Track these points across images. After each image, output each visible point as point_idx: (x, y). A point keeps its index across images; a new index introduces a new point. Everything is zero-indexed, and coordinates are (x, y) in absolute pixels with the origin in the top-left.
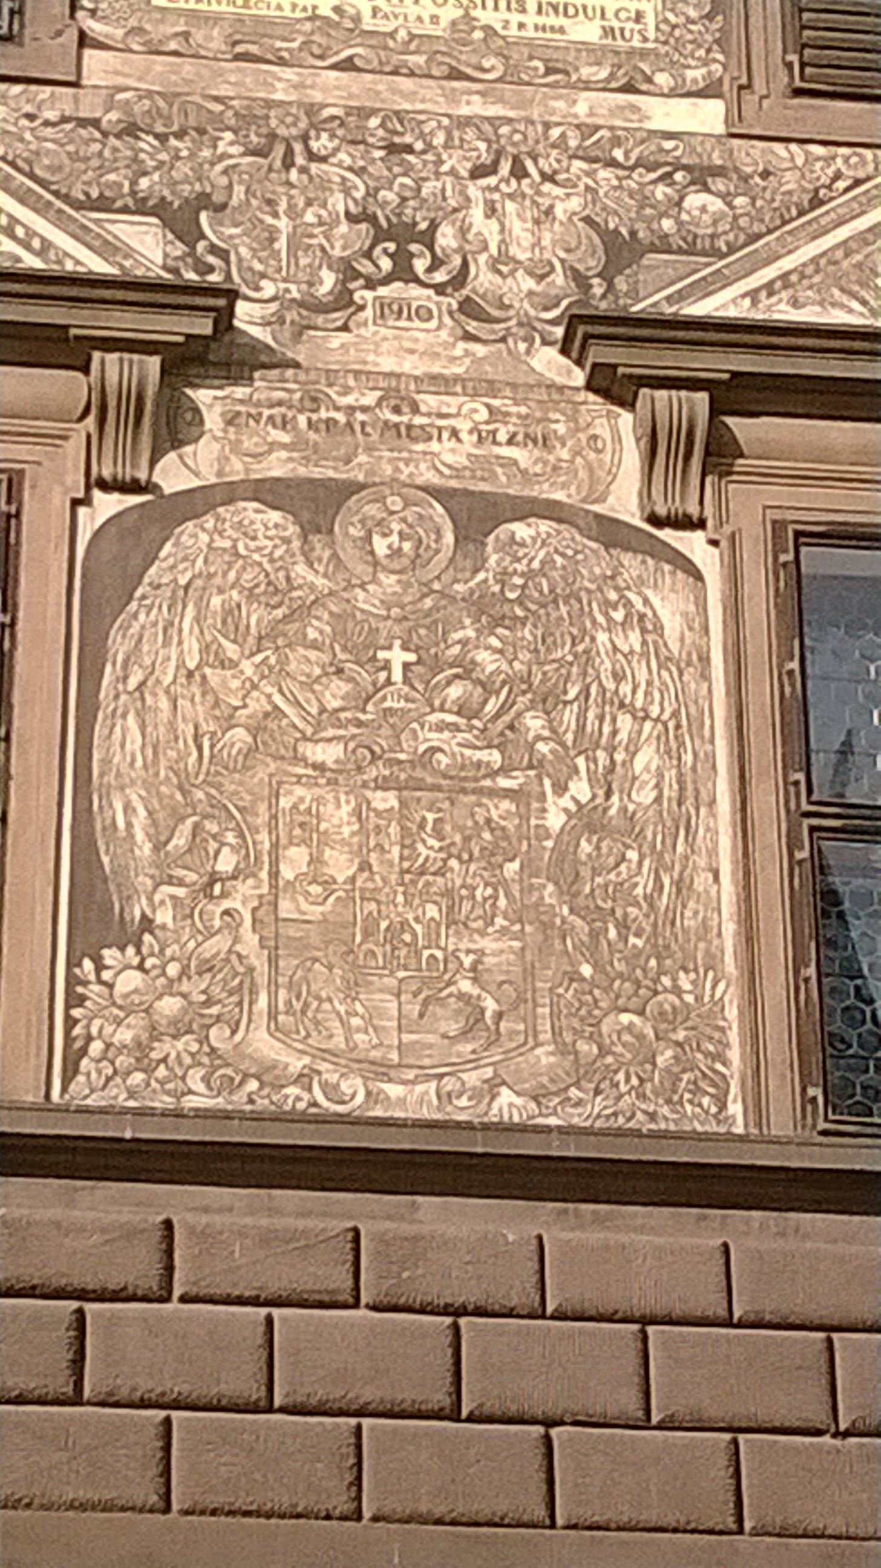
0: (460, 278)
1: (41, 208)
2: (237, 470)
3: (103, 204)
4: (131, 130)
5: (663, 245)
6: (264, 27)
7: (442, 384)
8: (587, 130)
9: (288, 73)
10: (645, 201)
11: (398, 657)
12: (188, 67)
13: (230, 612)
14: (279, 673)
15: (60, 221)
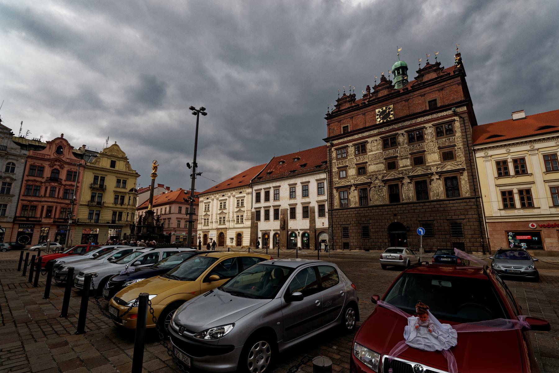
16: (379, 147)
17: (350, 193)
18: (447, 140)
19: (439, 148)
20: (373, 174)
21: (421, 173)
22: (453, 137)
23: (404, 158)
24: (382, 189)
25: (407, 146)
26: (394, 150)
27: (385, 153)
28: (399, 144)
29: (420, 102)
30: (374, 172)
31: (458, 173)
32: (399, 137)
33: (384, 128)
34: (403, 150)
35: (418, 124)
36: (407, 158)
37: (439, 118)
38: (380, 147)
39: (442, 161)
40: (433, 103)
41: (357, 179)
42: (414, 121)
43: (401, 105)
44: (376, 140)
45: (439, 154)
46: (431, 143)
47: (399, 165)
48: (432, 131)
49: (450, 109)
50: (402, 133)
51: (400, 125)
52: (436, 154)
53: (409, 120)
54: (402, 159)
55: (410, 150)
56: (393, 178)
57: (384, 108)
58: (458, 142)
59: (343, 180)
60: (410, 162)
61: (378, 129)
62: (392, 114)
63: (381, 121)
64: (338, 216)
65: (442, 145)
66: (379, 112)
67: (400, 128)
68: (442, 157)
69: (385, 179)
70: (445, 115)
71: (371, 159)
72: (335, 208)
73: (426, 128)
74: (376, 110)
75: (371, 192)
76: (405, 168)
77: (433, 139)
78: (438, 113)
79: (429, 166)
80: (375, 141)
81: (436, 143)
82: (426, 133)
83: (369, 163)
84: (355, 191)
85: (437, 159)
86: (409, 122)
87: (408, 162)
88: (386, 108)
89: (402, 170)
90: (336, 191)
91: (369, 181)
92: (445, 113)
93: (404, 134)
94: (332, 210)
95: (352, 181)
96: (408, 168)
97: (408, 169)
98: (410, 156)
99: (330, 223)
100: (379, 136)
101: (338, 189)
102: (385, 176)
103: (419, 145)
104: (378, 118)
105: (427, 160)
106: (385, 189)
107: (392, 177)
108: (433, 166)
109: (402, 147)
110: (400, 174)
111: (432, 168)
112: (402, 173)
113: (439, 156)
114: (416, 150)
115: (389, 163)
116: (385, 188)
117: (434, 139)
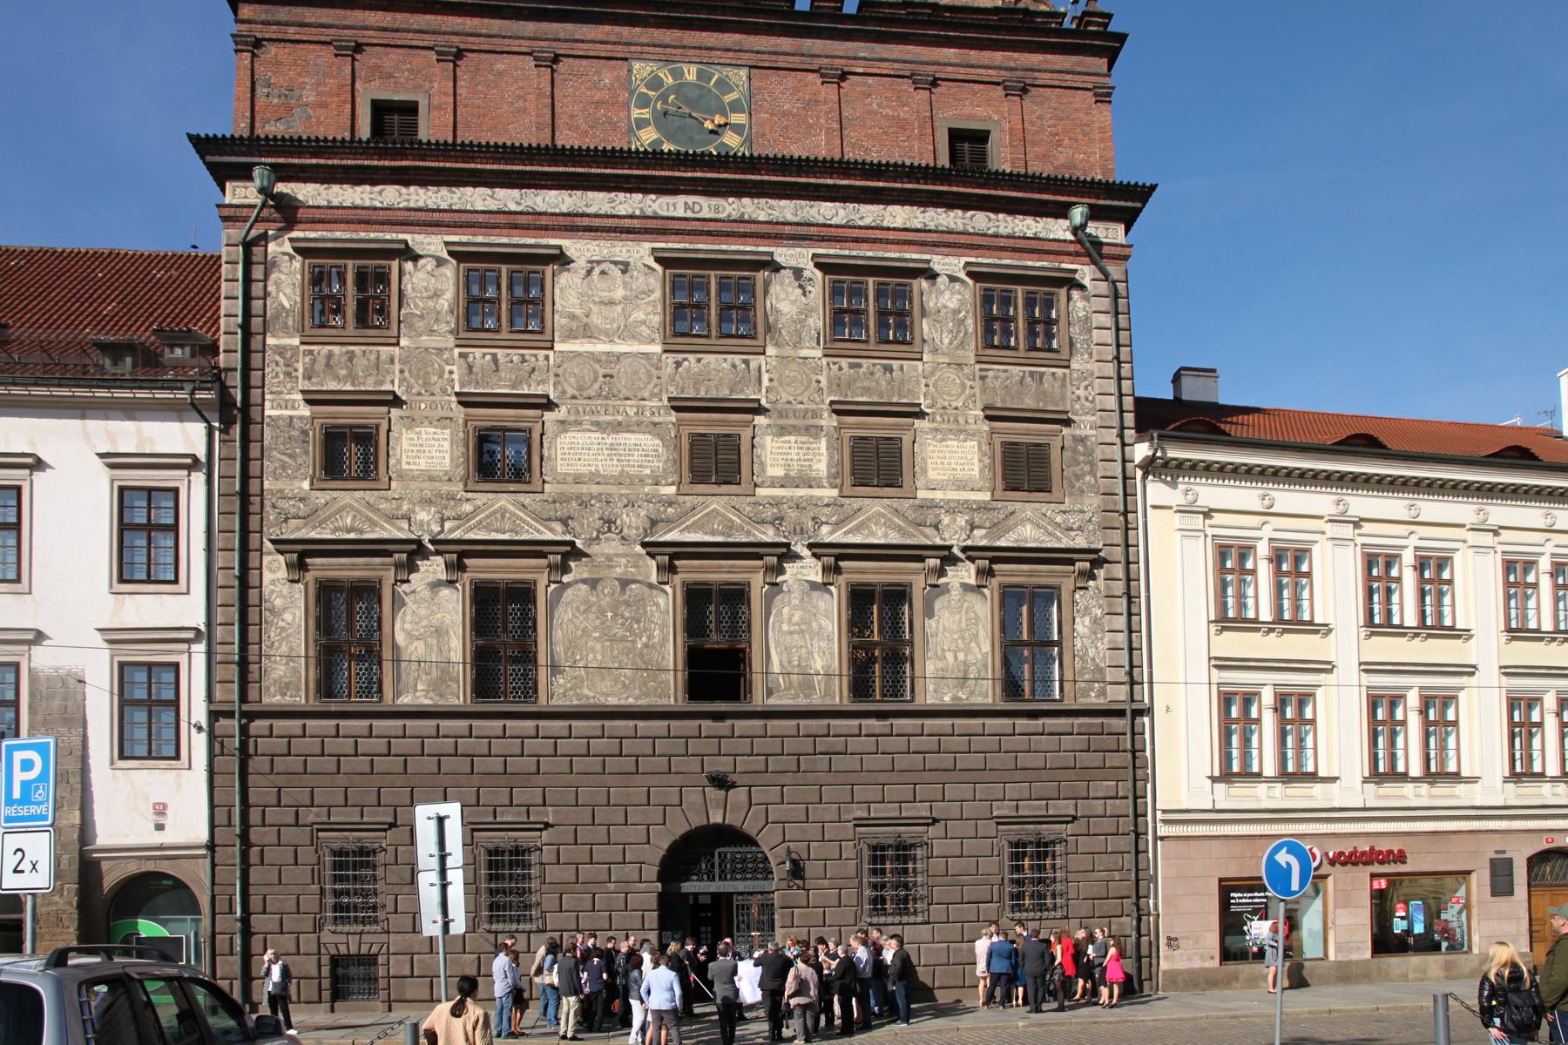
0: (621, 531)
1: (537, 521)
2: (578, 577)
3: (549, 520)
4: (554, 502)
5: (662, 521)
6: (581, 475)
7: (618, 555)
8: (647, 495)
9: (585, 486)
10: (658, 510)
11: (609, 614)
12: (565, 487)
13: (578, 608)
14: (586, 619)
15: (541, 524)
16: (640, 315)
17: (398, 603)
18: (1029, 379)
19: (993, 415)
20: (584, 489)
21: (886, 536)
22: (1059, 371)
23: (794, 430)
24: (640, 601)
25: (818, 353)
26: (737, 359)
27: (678, 364)
28: (769, 328)
29: (903, 113)
30: (596, 479)
31: (1067, 575)
32: (775, 289)
33: (681, 199)
34: (790, 371)
35: (891, 235)
36: (812, 431)
37: (1002, 242)
38: (650, 313)
39: (999, 494)
40: (967, 141)
41: (468, 508)
42: (868, 214)
43: (796, 90)
44: (625, 267)
45: (985, 447)
46: (951, 374)
47: (762, 464)
48: (962, 302)
49: (1061, 211)
50: (793, 263)
51: (786, 210)
52: (972, 445)
53: (844, 200)
54: (782, 431)
55: (836, 384)
56: (720, 539)
57: (691, 73)
58: (1077, 407)
59: (346, 498)
60: (831, 457)
61: (646, 192)
62: (738, 129)
63: (666, 147)
64: (295, 763)
65: (1003, 401)
66: (655, 83)
67: (787, 229)
68: (999, 469)
69: (668, 537)
70: (1030, 234)
71: (581, 388)
72: (273, 699)
73: (932, 276)
74: (637, 65)
75: (564, 614)
76: (801, 492)
77: (960, 352)
78: (996, 211)
79: (931, 505)
80: (616, 271)
81: (978, 382)
82: (931, 304)
83: (561, 413)
84: (445, 592)
85: (976, 472)
86: (842, 213)
87: (820, 457)
88: (701, 75)
89: (777, 502)
90: (283, 573)
91: (549, 536)
92: (1027, 226)
93: (807, 274)
94: (251, 716)
95: (422, 515)
96: (816, 492)
97: (814, 503)
98: (829, 421)
99: (221, 817)
100: (648, 246)
101: (301, 555)
102: (668, 521)
103: (889, 369)
104: (642, 123)
105: (924, 471)
106: (665, 607)
107: (713, 533)
108: (953, 508)
109: (788, 351)
110: (763, 522)
111: (946, 520)
112: (777, 521)
113: (987, 461)
114: (867, 390)
115: (698, 441)
116: (661, 601)
117: (970, 356)
